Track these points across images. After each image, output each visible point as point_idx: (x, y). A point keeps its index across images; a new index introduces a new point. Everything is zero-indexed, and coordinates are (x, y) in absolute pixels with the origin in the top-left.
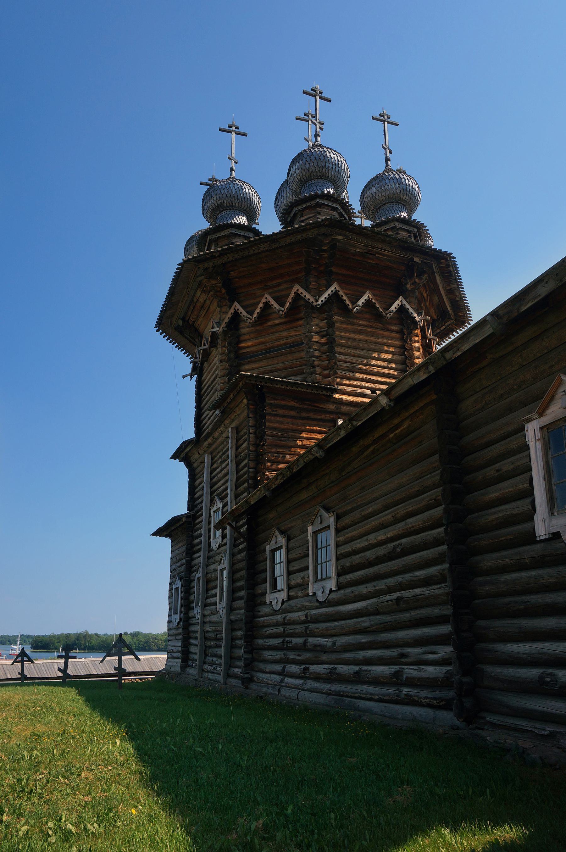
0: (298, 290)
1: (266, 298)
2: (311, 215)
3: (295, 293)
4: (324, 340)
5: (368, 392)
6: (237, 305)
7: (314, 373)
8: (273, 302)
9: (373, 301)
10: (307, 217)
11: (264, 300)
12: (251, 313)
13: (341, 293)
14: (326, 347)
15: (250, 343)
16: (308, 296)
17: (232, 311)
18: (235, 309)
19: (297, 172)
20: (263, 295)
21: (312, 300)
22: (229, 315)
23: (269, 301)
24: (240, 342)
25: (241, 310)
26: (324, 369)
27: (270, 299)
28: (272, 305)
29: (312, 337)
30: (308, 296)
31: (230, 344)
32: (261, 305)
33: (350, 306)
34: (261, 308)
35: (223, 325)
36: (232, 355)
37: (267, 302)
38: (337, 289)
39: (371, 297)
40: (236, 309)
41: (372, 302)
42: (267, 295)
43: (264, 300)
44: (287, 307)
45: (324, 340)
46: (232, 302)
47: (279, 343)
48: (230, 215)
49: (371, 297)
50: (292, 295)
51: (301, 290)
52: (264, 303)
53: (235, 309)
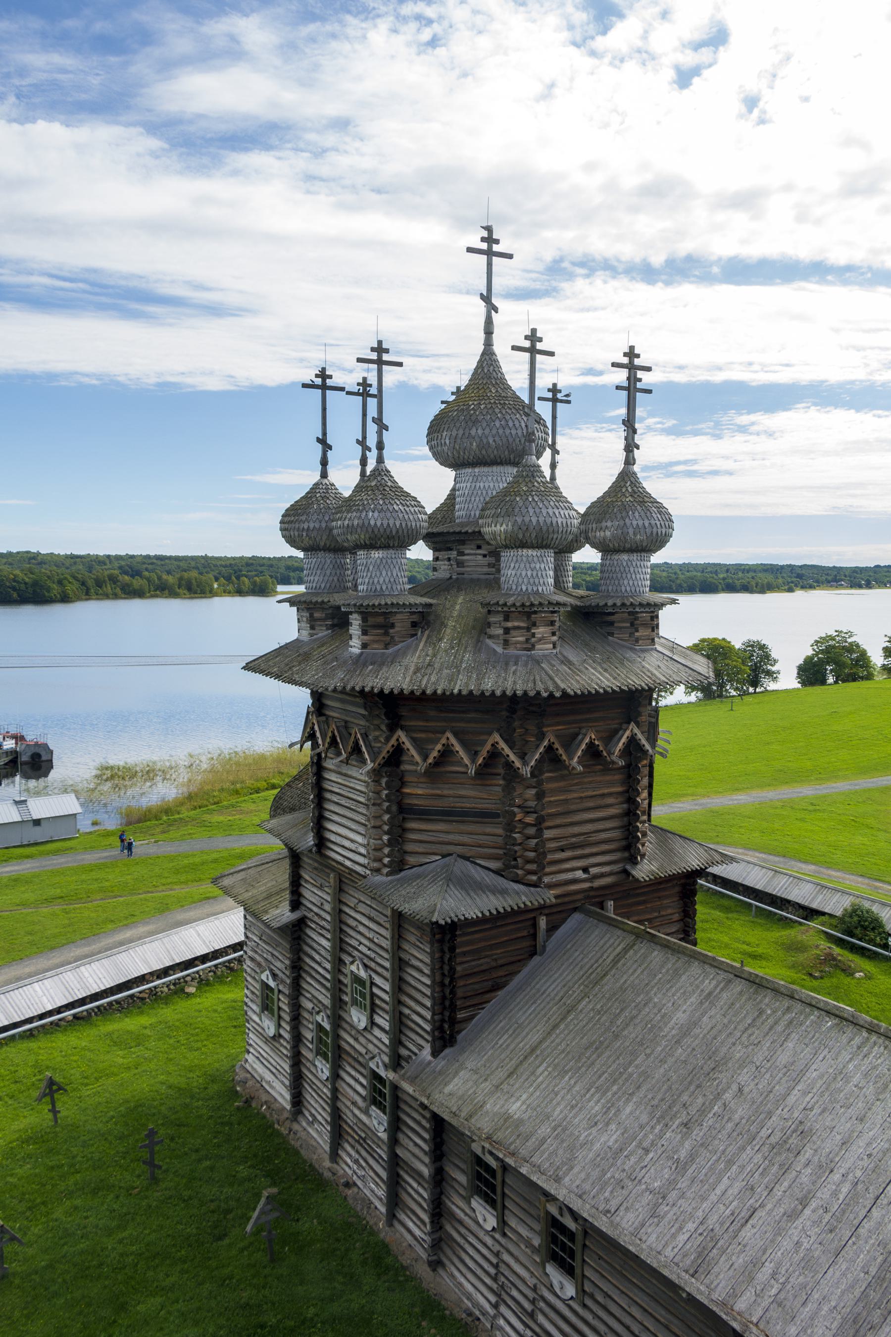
0: (497, 743)
1: (448, 739)
2: (522, 624)
3: (493, 745)
4: (530, 819)
5: (579, 874)
6: (401, 735)
7: (516, 867)
8: (458, 747)
9: (597, 743)
10: (516, 624)
11: (443, 741)
12: (425, 757)
13: (557, 746)
14: (532, 831)
15: (420, 792)
16: (512, 757)
17: (393, 741)
18: (398, 740)
19: (503, 537)
20: (444, 733)
21: (518, 764)
22: (388, 747)
23: (452, 745)
24: (403, 784)
25: (408, 745)
26: (528, 862)
27: (453, 741)
28: (457, 752)
29: (515, 815)
30: (512, 757)
31: (388, 786)
32: (439, 747)
33: (567, 763)
34: (439, 751)
35: (379, 760)
36: (394, 808)
37: (448, 745)
38: (552, 740)
39: (593, 737)
40: (401, 741)
41: (594, 744)
42: (449, 735)
43: (443, 741)
44: (480, 762)
45: (530, 819)
46: (392, 729)
47: (463, 805)
48: (384, 561)
49: (593, 737)
50: (488, 747)
51: (502, 745)
52: (444, 745)
53: (398, 740)
